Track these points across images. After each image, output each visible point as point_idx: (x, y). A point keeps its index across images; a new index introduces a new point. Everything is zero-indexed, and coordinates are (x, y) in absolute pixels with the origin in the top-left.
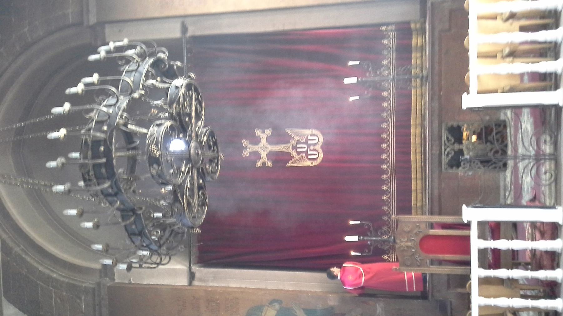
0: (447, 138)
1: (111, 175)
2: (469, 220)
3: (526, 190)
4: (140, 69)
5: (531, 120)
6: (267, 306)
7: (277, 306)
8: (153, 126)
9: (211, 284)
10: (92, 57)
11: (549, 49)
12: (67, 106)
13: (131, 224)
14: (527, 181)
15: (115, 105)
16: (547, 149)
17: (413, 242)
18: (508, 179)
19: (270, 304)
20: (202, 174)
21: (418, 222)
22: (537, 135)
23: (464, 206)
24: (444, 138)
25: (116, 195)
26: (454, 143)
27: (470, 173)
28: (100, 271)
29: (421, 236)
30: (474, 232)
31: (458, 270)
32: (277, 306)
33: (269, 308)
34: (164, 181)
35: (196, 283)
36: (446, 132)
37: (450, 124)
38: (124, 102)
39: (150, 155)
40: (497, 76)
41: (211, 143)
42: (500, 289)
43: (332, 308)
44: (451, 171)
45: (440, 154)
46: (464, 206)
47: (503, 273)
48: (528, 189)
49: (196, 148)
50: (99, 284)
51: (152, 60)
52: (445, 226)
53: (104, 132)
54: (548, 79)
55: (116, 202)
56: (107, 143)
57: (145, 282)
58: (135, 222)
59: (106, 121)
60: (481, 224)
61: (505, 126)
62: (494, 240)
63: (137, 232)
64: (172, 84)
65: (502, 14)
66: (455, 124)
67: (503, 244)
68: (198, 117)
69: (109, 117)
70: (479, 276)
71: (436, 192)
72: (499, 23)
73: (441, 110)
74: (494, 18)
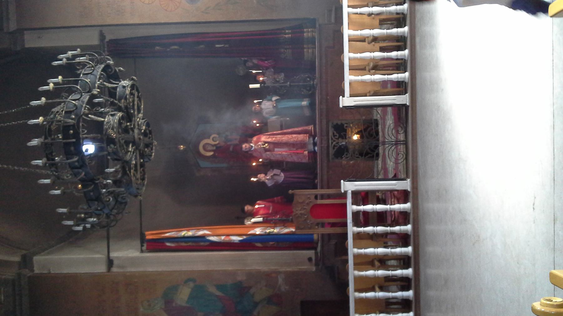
0: (333, 133)
2: (346, 190)
3: (390, 172)
4: (95, 72)
5: (393, 117)
7: (192, 284)
8: (109, 116)
9: (129, 269)
10: (56, 63)
11: (402, 63)
12: (43, 99)
13: (90, 191)
14: (390, 164)
15: (78, 99)
16: (401, 137)
17: (305, 211)
18: (380, 166)
20: (142, 156)
21: (309, 194)
22: (396, 127)
23: (342, 181)
24: (331, 134)
25: (81, 167)
26: (338, 139)
27: (351, 162)
28: (19, 263)
29: (311, 205)
30: (349, 200)
31: (338, 230)
34: (118, 158)
35: (114, 269)
36: (333, 129)
37: (335, 123)
38: (86, 97)
39: (108, 136)
40: (363, 82)
41: (148, 131)
42: (370, 242)
43: (241, 282)
44: (337, 160)
45: (328, 147)
46: (342, 181)
47: (370, 229)
48: (392, 171)
49: (139, 135)
50: (19, 275)
51: (103, 66)
52: (329, 197)
53: (72, 119)
54: (401, 86)
55: (82, 173)
56: (75, 127)
57: (65, 271)
58: (92, 191)
59: (73, 111)
60: (355, 194)
61: (377, 125)
62: (363, 206)
64: (120, 84)
65: (368, 37)
66: (339, 123)
67: (369, 207)
68: (139, 111)
69: (77, 108)
70: (353, 232)
71: (325, 177)
72: (365, 44)
74: (363, 41)
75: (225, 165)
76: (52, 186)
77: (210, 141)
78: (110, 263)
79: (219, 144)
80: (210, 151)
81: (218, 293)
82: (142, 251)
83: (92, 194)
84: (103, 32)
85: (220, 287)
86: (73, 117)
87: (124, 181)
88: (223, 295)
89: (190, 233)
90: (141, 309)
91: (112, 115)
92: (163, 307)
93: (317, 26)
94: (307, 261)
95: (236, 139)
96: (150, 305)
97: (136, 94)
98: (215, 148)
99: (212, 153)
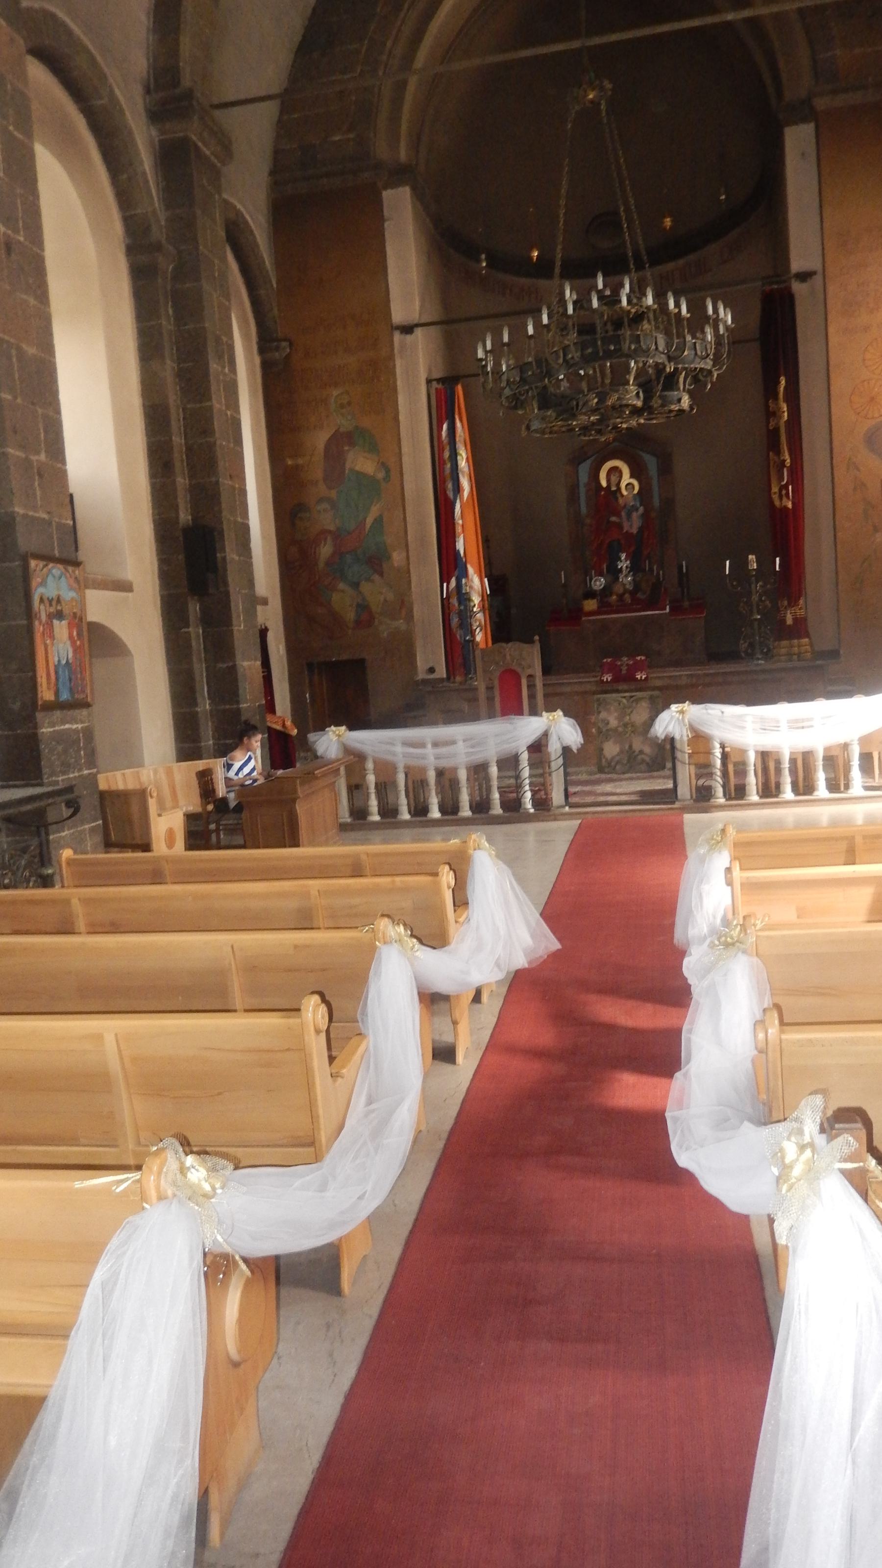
1: (587, 360)
4: (698, 360)
6: (379, 460)
7: (381, 475)
9: (398, 363)
15: (657, 349)
19: (383, 464)
25: (565, 360)
27: (594, 730)
32: (381, 475)
33: (375, 464)
34: (580, 408)
35: (397, 337)
43: (389, 558)
63: (525, 376)
73: (677, 687)
75: (584, 509)
76: (538, 324)
77: (626, 479)
78: (408, 329)
79: (622, 496)
80: (608, 481)
81: (369, 521)
82: (429, 382)
83: (530, 373)
84: (814, 277)
85: (379, 521)
86: (633, 347)
87: (549, 413)
88: (367, 530)
89: (463, 464)
90: (335, 393)
91: (638, 393)
92: (341, 430)
93: (819, 662)
94: (431, 665)
95: (631, 526)
96: (342, 406)
97: (672, 415)
98: (614, 488)
99: (604, 483)
